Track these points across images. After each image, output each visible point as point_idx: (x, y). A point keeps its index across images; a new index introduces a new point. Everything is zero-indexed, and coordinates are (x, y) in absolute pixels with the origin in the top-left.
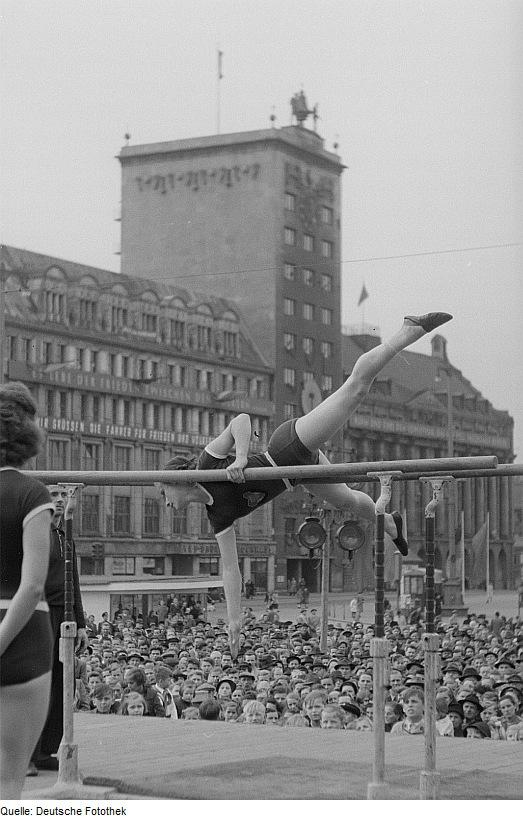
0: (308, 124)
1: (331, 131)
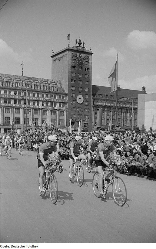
0: (82, 45)
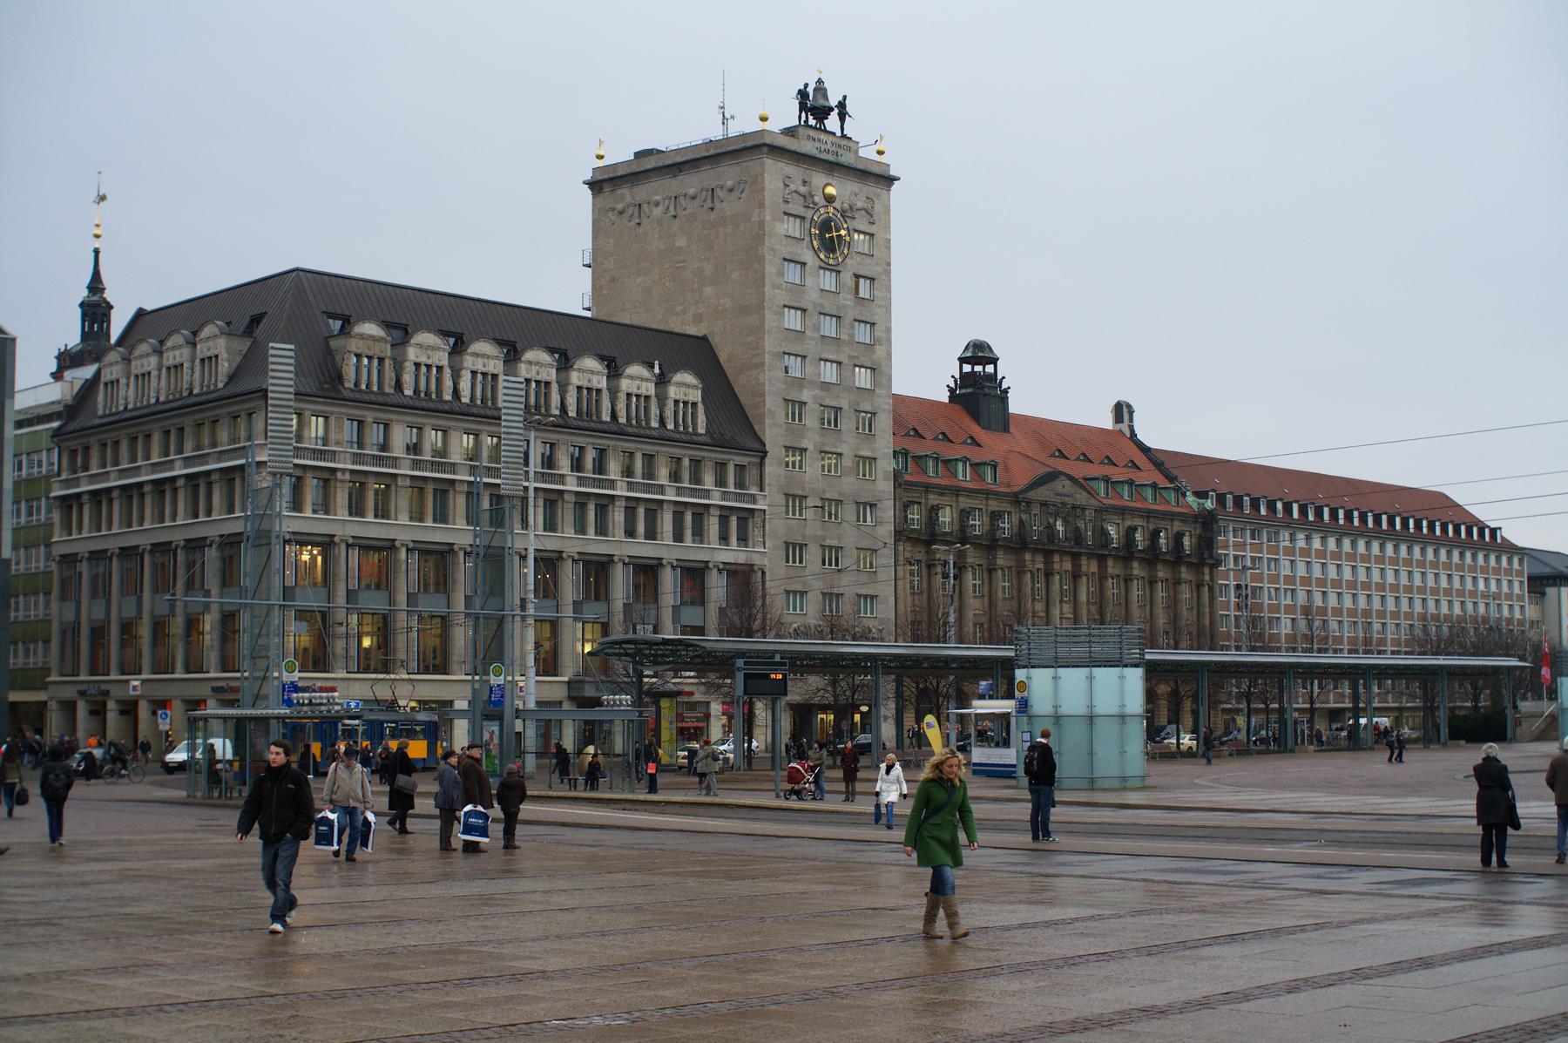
0: (832, 122)
1: (866, 132)
